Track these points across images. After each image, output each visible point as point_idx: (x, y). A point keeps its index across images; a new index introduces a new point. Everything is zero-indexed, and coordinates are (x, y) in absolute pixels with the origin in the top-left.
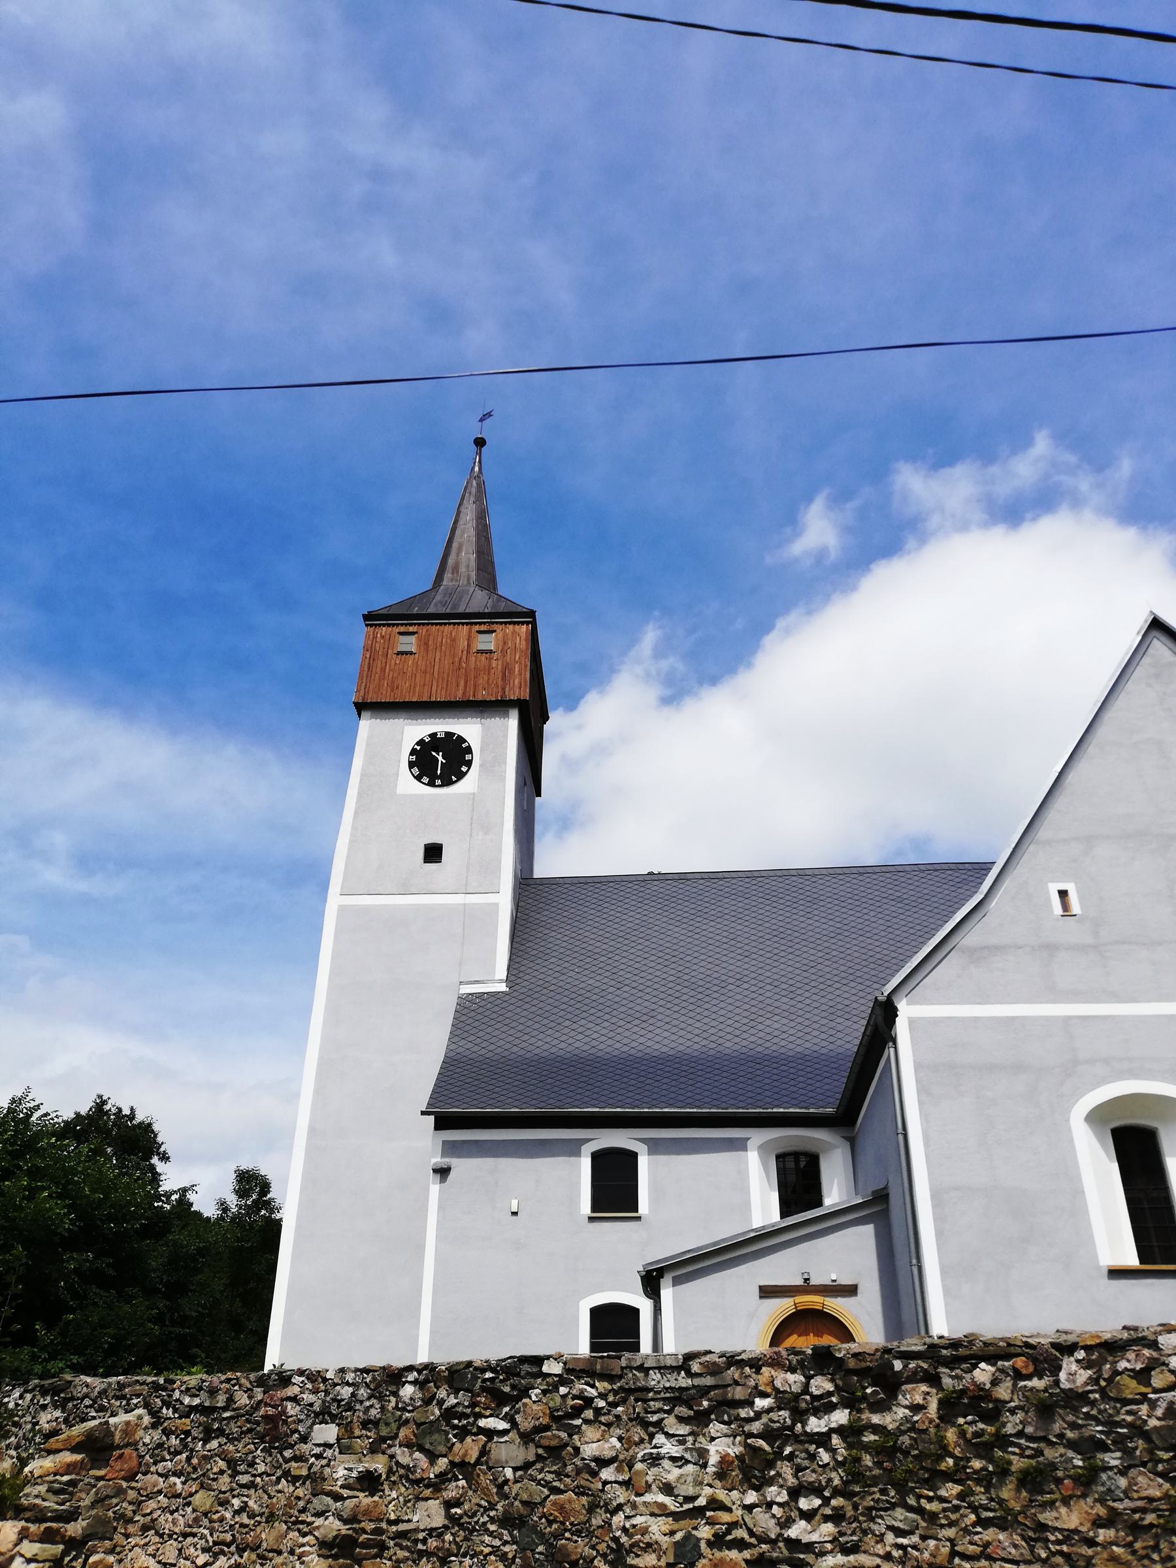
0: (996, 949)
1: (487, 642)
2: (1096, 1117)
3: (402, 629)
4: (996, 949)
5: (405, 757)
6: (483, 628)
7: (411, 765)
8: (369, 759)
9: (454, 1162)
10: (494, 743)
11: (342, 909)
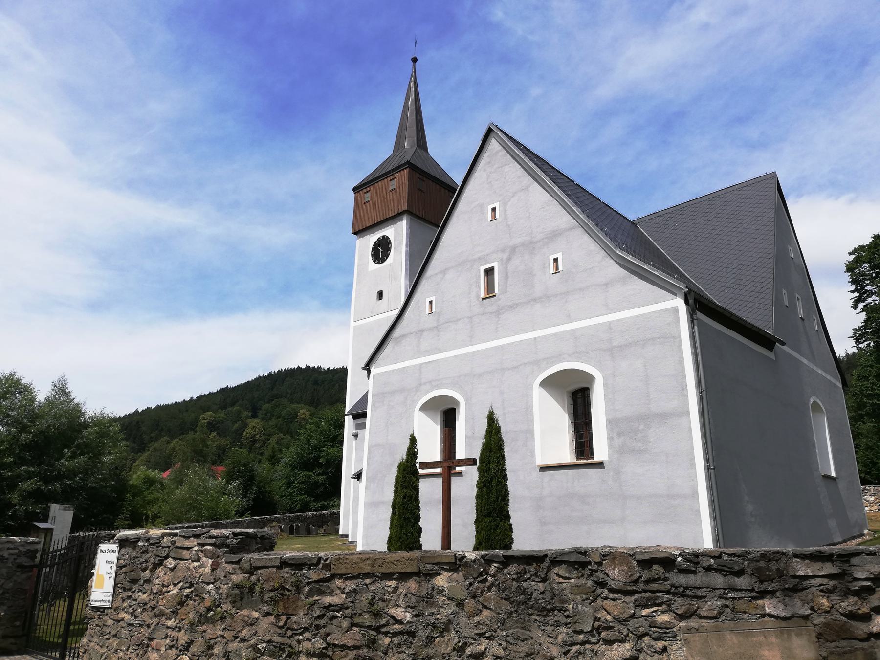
0: (403, 336)
1: (393, 185)
2: (425, 408)
3: (366, 190)
4: (403, 336)
6: (391, 178)
7: (372, 256)
8: (360, 259)
9: (360, 432)
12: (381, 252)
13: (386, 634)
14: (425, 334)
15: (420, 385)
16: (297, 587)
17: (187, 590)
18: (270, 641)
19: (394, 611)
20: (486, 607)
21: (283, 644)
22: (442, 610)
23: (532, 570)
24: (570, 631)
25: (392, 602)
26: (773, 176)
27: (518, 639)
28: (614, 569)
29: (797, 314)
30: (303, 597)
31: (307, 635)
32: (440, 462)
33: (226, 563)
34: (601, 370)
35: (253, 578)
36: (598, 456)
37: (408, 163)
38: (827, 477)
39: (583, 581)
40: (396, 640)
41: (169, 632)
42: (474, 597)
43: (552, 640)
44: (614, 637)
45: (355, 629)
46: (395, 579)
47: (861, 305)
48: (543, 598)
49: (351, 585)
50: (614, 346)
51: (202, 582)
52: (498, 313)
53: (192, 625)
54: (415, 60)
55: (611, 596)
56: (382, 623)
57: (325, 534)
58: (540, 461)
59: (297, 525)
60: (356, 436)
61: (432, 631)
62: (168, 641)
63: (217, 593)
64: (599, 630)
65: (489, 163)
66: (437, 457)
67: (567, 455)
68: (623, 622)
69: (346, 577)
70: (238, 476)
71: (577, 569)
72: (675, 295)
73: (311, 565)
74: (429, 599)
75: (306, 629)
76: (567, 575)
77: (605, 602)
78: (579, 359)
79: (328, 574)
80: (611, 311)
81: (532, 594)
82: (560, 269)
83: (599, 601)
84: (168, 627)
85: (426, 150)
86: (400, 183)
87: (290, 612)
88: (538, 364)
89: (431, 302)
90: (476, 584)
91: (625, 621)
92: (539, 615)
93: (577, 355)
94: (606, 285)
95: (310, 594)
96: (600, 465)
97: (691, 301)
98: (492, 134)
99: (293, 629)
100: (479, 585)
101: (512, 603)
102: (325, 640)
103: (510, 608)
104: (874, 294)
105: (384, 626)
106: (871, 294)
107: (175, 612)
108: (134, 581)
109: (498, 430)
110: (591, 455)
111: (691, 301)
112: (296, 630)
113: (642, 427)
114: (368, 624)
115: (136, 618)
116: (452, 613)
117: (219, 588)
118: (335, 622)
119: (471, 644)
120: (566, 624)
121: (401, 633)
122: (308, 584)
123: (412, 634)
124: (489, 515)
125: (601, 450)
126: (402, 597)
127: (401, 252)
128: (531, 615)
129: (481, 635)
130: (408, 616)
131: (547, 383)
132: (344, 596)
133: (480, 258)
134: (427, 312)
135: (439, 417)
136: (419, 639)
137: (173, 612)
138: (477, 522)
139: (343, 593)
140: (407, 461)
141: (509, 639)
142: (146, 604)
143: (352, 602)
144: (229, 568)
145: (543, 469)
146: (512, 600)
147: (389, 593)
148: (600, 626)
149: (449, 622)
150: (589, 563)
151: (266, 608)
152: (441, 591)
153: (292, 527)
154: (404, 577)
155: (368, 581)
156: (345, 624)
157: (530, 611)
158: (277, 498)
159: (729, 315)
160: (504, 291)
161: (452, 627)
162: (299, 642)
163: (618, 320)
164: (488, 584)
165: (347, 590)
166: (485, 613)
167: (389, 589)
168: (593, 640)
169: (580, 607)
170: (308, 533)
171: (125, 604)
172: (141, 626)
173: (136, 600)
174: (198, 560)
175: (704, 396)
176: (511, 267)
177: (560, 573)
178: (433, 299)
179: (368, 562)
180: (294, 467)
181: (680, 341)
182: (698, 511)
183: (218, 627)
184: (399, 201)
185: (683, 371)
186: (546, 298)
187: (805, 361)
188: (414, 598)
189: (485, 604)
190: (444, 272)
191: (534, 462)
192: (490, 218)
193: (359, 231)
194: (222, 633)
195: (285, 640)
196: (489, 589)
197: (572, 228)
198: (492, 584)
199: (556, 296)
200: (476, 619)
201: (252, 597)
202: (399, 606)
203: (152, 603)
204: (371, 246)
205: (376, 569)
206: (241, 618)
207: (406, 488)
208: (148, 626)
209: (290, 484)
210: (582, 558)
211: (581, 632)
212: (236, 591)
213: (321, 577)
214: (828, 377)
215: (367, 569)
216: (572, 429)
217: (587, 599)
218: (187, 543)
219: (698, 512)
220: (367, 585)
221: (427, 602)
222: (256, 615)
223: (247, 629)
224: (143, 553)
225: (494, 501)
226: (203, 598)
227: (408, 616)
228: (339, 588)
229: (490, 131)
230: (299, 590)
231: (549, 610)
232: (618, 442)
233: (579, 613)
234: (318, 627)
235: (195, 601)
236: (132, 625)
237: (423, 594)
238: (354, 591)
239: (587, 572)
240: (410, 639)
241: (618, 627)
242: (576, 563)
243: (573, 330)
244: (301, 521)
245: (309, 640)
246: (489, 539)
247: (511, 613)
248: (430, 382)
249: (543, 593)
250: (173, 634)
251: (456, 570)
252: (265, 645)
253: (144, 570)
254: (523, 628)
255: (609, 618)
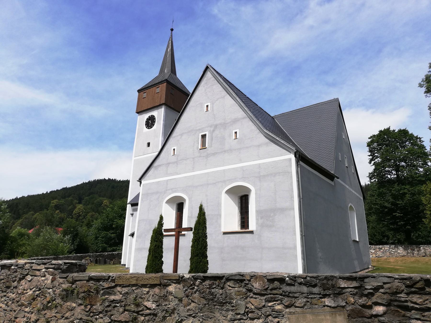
0: (160, 166)
1: (158, 90)
2: (168, 202)
3: (144, 92)
4: (160, 166)
5: (145, 123)
7: (146, 125)
9: (134, 212)
10: (159, 115)
11: (135, 160)
12: (150, 123)
13: (142, 315)
14: (170, 165)
15: (167, 190)
16: (97, 291)
17: (37, 292)
18: (81, 319)
19: (146, 303)
20: (193, 302)
21: (88, 320)
22: (171, 303)
23: (217, 283)
24: (234, 313)
25: (146, 299)
26: (337, 100)
27: (208, 317)
28: (256, 283)
29: (345, 165)
30: (100, 296)
31: (101, 315)
32: (174, 229)
33: (60, 278)
34: (254, 187)
35: (74, 286)
36: (251, 228)
37: (166, 80)
38: (355, 241)
39: (241, 289)
40: (147, 318)
41: (26, 314)
42: (187, 296)
43: (225, 318)
44: (255, 317)
45: (126, 312)
46: (148, 287)
47: (373, 162)
48: (222, 297)
49: (125, 290)
50: (261, 176)
51: (46, 288)
52: (207, 156)
53: (39, 310)
54: (172, 30)
55: (254, 296)
56: (140, 309)
57: (114, 264)
58: (224, 230)
59: (99, 259)
60: (132, 215)
61: (166, 313)
62: (25, 319)
63: (54, 294)
64: (247, 313)
65: (206, 83)
66: (173, 226)
67: (237, 227)
68: (259, 309)
69: (123, 286)
70: (70, 233)
71: (239, 283)
72: (290, 152)
73: (105, 280)
74: (165, 297)
75: (100, 313)
76: (234, 286)
77: (251, 299)
78: (244, 181)
79: (113, 284)
80: (260, 159)
81: (216, 295)
82: (238, 137)
83: (248, 299)
84: (25, 312)
85: (175, 74)
86: (162, 89)
87: (93, 303)
88: (225, 182)
89: (174, 149)
90: (189, 290)
91: (261, 308)
92: (219, 306)
93: (244, 179)
94: (259, 146)
95: (103, 294)
96: (252, 232)
97: (297, 156)
98: (208, 70)
99: (93, 313)
100: (190, 290)
101: (206, 300)
102: (110, 318)
103: (205, 302)
104: (378, 157)
105: (141, 311)
106: (377, 157)
107: (30, 304)
108: (8, 287)
109: (204, 214)
110: (248, 227)
111: (297, 156)
112: (95, 313)
113: (272, 215)
114: (133, 310)
115: (8, 306)
116: (176, 305)
117: (55, 291)
118: (116, 309)
119: (185, 320)
120: (232, 310)
121: (150, 314)
122: (103, 289)
123: (155, 315)
124: (197, 255)
125: (252, 226)
126: (151, 296)
127: (161, 124)
128: (215, 305)
129: (190, 315)
130: (154, 306)
131: (228, 192)
132: (121, 296)
133: (199, 129)
134: (172, 154)
135: (175, 207)
136: (159, 318)
137: (29, 304)
138: (191, 259)
139: (121, 294)
140: (158, 228)
141: (204, 317)
142: (14, 299)
143: (125, 299)
144: (61, 280)
145: (225, 233)
146: (206, 298)
147: (145, 294)
148: (248, 311)
149: (175, 309)
150: (245, 280)
151: (80, 302)
152: (171, 293)
153: (97, 260)
154: (153, 286)
155: (134, 288)
156: (121, 310)
157: (215, 303)
158: (90, 244)
159: (314, 163)
160: (211, 146)
161: (176, 312)
162: (96, 319)
163: (264, 163)
164: (195, 290)
165: (123, 293)
166: (193, 304)
167: (145, 292)
168: (245, 318)
169: (239, 302)
170: (105, 263)
171: (3, 299)
172: (11, 311)
173: (8, 297)
174: (45, 276)
175: (301, 201)
176: (214, 135)
177: (230, 285)
178: (175, 148)
179: (135, 278)
180: (99, 230)
181: (292, 174)
182: (296, 256)
183: (53, 312)
184: (161, 99)
185: (292, 189)
186: (230, 150)
187: (347, 187)
188: (157, 297)
189: (193, 300)
190: (182, 135)
191: (220, 230)
192: (205, 110)
193: (139, 112)
194: (55, 315)
195: (89, 318)
196: (195, 292)
197: (244, 118)
198: (197, 290)
199: (235, 150)
200: (188, 308)
201: (73, 296)
202: (149, 301)
203: (17, 299)
204: (145, 120)
205: (138, 282)
206: (66, 307)
207: (157, 241)
208: (15, 311)
209: (96, 238)
210: (241, 278)
211: (239, 314)
212: (64, 293)
213: (110, 286)
214: (357, 195)
215: (134, 282)
216: (239, 215)
217: (242, 298)
218: (39, 267)
219: (296, 256)
220: (133, 290)
221: (164, 299)
222: (74, 305)
223: (69, 312)
224: (14, 272)
225: (200, 249)
226: (46, 296)
227: (154, 306)
228: (119, 292)
229: (207, 68)
230: (98, 292)
231: (224, 303)
232: (261, 221)
233: (239, 305)
234: (107, 311)
235: (41, 298)
236: (6, 310)
237: (162, 295)
238: (127, 293)
239: (243, 284)
240: (154, 317)
241: (257, 311)
242: (238, 280)
243: (243, 167)
244: (102, 257)
245: (102, 318)
246: (196, 267)
247: (205, 305)
248: (172, 189)
249: (221, 294)
250: (28, 315)
251: (179, 283)
252: (78, 321)
253: (14, 282)
254: (211, 312)
255: (253, 307)
